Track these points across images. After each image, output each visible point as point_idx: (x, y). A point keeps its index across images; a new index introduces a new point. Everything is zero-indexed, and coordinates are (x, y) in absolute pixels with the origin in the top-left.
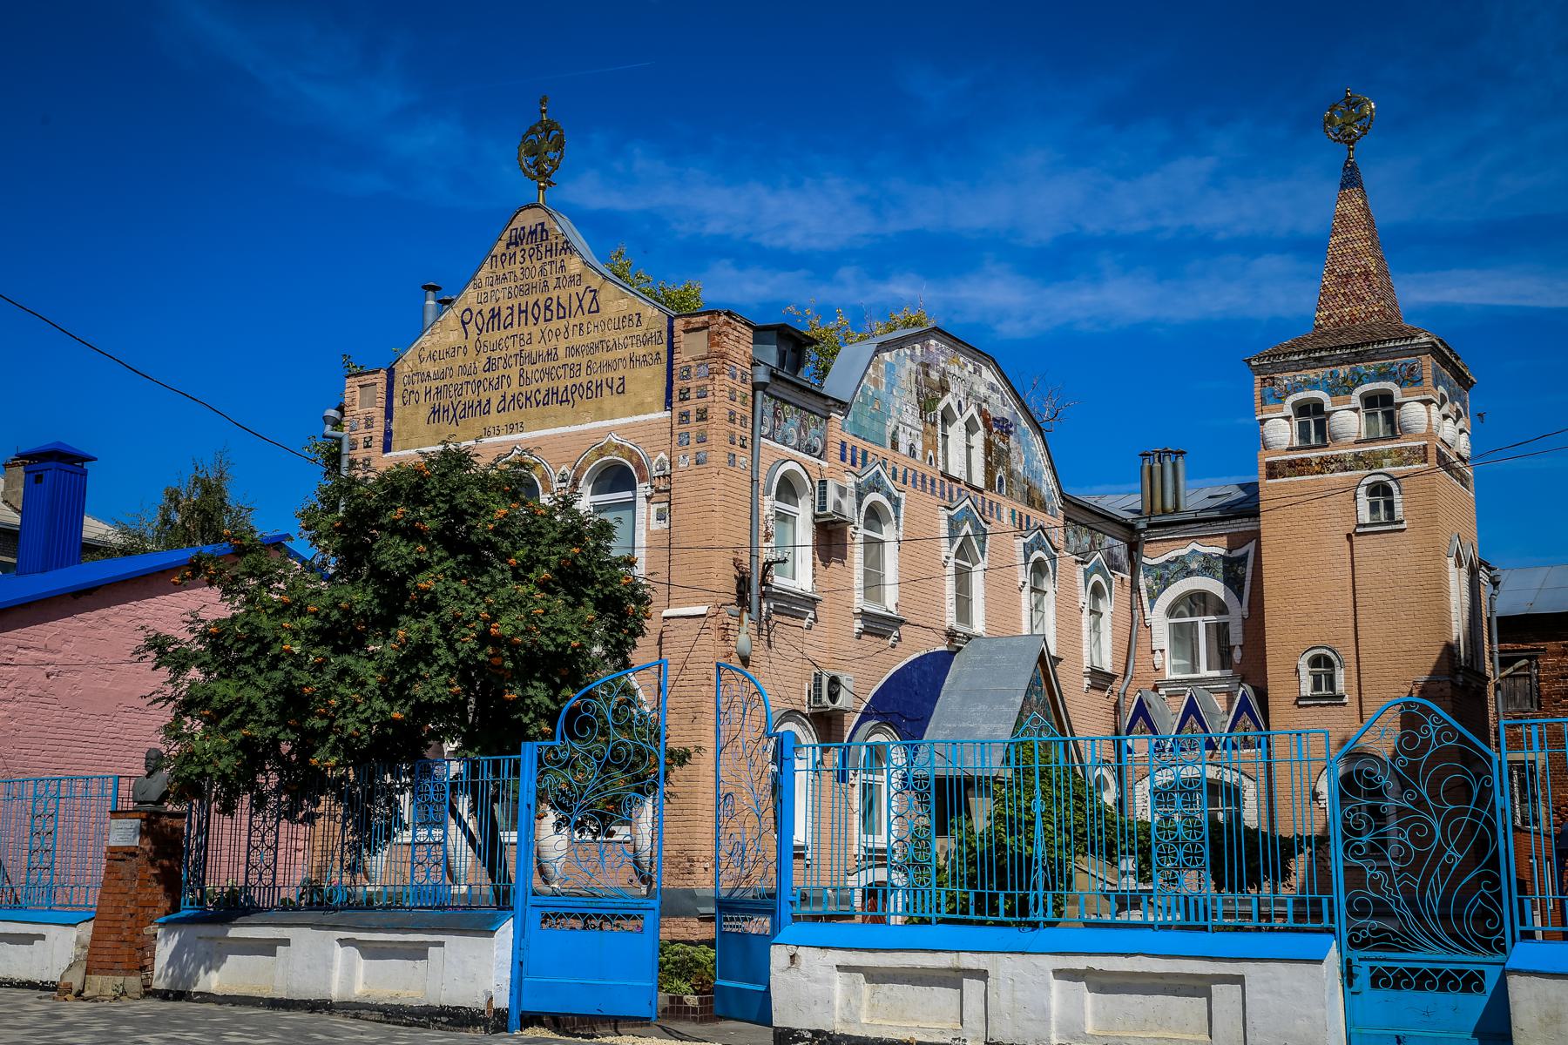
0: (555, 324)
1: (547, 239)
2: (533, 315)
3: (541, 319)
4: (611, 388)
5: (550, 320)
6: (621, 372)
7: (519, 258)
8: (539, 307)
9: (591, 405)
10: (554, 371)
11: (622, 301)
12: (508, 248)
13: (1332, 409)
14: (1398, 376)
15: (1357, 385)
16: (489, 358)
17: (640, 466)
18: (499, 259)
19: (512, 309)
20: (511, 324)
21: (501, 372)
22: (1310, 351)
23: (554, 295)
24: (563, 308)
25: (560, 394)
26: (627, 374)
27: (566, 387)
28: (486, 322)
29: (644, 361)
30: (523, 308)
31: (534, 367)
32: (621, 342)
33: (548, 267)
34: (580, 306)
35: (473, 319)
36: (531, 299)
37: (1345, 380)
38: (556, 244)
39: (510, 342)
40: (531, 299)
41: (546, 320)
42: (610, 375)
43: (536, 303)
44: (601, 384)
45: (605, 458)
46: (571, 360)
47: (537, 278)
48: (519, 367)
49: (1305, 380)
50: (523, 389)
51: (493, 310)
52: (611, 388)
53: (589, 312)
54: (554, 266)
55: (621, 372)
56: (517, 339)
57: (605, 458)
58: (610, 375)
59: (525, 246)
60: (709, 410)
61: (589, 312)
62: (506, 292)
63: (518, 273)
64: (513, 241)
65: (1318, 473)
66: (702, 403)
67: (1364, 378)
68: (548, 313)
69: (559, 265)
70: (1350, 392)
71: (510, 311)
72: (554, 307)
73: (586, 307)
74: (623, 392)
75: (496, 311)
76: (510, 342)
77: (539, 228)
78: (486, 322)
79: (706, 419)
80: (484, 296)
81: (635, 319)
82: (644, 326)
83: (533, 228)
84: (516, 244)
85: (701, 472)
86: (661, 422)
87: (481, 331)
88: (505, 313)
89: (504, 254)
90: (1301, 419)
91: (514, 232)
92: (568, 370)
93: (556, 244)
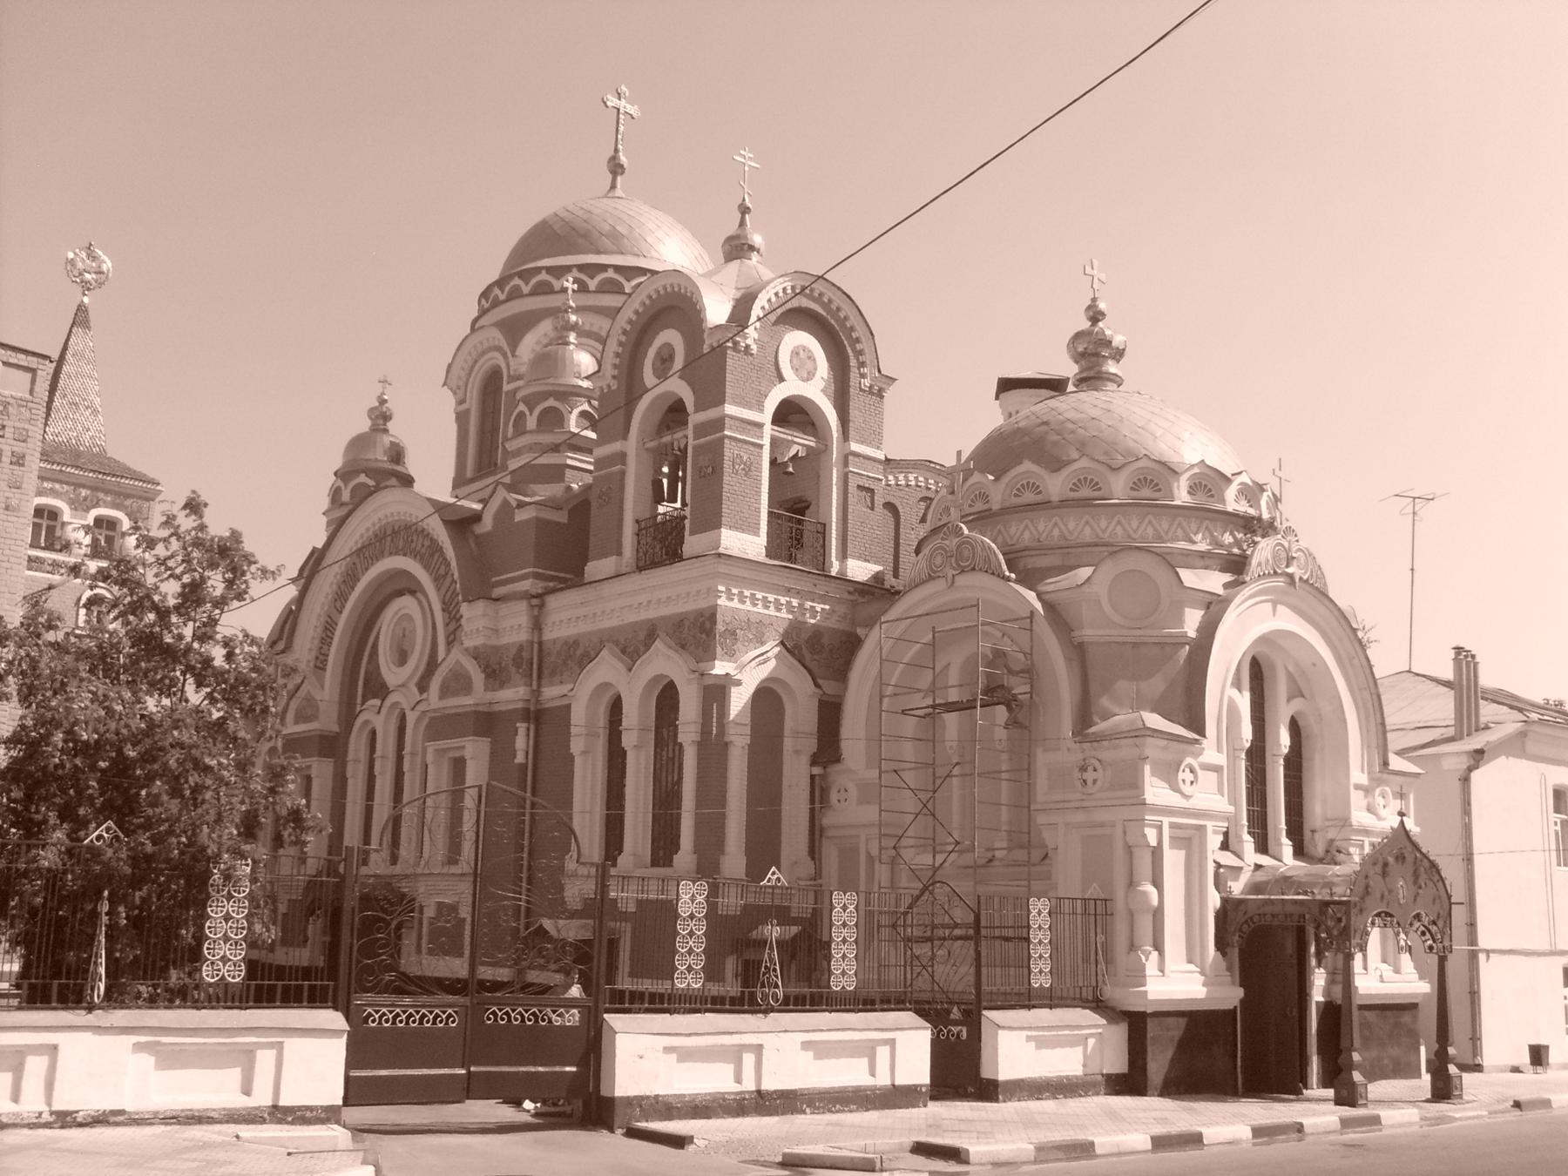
13: (70, 520)
14: (129, 510)
15: (94, 507)
22: (64, 465)
37: (85, 499)
49: (51, 489)
65: (48, 572)
66: (19, 448)
67: (101, 503)
70: (88, 510)
79: (23, 465)
85: (10, 518)
90: (36, 520)
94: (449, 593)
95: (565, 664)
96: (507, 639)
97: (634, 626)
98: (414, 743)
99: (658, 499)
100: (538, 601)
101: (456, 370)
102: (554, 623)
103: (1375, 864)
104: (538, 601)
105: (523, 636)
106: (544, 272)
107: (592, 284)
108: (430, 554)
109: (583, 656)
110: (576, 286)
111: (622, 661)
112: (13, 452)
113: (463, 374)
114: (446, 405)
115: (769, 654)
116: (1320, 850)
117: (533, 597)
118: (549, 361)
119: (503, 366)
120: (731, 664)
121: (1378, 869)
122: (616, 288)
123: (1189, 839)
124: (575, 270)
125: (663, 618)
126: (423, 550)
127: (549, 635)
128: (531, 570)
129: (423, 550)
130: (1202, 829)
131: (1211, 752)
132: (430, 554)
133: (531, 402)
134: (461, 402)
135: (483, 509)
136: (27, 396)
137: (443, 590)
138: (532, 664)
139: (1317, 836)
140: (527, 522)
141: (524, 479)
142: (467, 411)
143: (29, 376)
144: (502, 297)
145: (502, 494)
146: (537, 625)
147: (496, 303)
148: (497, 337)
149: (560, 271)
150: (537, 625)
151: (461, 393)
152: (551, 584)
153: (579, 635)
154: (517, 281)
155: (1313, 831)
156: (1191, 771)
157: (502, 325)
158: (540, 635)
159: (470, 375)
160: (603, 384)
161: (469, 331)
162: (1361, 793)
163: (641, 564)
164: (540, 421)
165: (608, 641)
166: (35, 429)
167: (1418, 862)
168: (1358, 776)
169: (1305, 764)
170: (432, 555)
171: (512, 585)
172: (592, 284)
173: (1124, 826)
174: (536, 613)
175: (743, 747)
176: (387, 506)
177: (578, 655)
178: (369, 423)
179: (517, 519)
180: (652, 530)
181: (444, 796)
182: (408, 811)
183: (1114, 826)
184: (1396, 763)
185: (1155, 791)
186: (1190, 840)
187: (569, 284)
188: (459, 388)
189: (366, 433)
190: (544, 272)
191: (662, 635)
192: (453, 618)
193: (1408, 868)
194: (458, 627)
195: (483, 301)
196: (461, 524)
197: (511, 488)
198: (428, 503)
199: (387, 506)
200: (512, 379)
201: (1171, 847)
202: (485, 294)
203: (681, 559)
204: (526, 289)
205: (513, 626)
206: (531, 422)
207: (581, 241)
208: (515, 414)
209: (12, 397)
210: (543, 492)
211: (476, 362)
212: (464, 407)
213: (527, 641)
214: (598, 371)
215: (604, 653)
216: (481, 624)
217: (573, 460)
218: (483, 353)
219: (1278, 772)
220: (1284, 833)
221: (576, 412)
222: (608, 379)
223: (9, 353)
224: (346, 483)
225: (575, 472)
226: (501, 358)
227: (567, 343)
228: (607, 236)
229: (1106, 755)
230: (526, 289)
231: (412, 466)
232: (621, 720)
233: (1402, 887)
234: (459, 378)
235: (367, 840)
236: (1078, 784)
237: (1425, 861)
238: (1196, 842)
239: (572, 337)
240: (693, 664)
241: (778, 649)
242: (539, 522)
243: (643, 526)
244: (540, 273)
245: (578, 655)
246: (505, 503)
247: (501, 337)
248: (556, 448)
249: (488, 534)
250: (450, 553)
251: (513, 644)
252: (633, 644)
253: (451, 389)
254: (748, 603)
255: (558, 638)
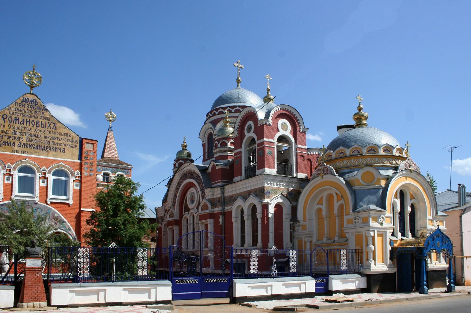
0: (40, 128)
1: (37, 105)
2: (34, 123)
3: (35, 126)
4: (61, 150)
5: (39, 127)
6: (64, 147)
7: (26, 106)
8: (34, 122)
9: (53, 153)
10: (40, 141)
11: (64, 129)
12: (22, 102)
16: (14, 131)
17: (72, 173)
18: (18, 104)
19: (24, 119)
20: (23, 124)
21: (19, 136)
23: (41, 120)
24: (43, 125)
25: (42, 147)
26: (66, 148)
27: (44, 147)
28: (13, 120)
29: (72, 146)
30: (28, 120)
31: (32, 138)
32: (64, 140)
33: (38, 113)
34: (50, 126)
35: (8, 118)
36: (32, 119)
38: (41, 107)
39: (22, 128)
40: (32, 119)
41: (37, 126)
42: (60, 147)
43: (33, 121)
44: (57, 148)
45: (60, 168)
46: (46, 140)
47: (33, 114)
48: (26, 137)
50: (28, 143)
51: (16, 118)
52: (61, 150)
53: (53, 129)
54: (40, 113)
55: (64, 147)
56: (26, 129)
57: (60, 168)
58: (60, 147)
59: (30, 105)
60: (94, 163)
61: (53, 129)
62: (21, 115)
63: (26, 111)
64: (24, 100)
68: (38, 125)
69: (42, 113)
71: (23, 120)
72: (40, 123)
73: (52, 127)
74: (65, 152)
75: (17, 118)
76: (23, 129)
77: (34, 101)
78: (13, 120)
79: (93, 165)
80: (12, 113)
81: (69, 135)
82: (72, 138)
83: (32, 100)
84: (26, 102)
86: (76, 162)
87: (11, 122)
88: (20, 120)
89: (20, 103)
91: (24, 99)
92: (45, 142)
93: (41, 107)
94: (202, 187)
95: (230, 201)
96: (216, 197)
97: (246, 192)
98: (190, 222)
99: (250, 161)
100: (223, 188)
101: (201, 133)
102: (227, 192)
103: (430, 238)
104: (223, 188)
105: (220, 196)
106: (221, 109)
107: (233, 111)
108: (197, 178)
109: (234, 199)
110: (228, 112)
111: (243, 200)
112: (90, 163)
113: (203, 135)
114: (200, 142)
115: (278, 197)
116: (419, 235)
117: (221, 186)
118: (222, 130)
119: (212, 131)
120: (269, 199)
121: (432, 239)
122: (238, 111)
123: (383, 234)
124: (228, 108)
125: (251, 190)
126: (195, 177)
127: (226, 195)
128: (220, 180)
129: (195, 177)
130: (386, 232)
131: (388, 213)
132: (197, 178)
133: (218, 140)
134: (203, 141)
135: (209, 166)
136: (92, 150)
137: (200, 186)
138: (222, 202)
139: (418, 232)
140: (219, 169)
141: (218, 159)
142: (205, 143)
143: (92, 145)
144: (211, 116)
145: (213, 163)
146: (223, 193)
147: (210, 117)
148: (210, 125)
149: (224, 108)
150: (223, 193)
151: (203, 139)
152: (226, 183)
153: (233, 195)
154: (214, 111)
155: (417, 231)
156: (383, 218)
157: (211, 122)
158: (224, 195)
159: (205, 135)
160: (235, 135)
161: (204, 124)
162: (430, 221)
163: (246, 177)
164: (221, 145)
165: (240, 196)
166: (94, 157)
167: (443, 237)
168: (429, 217)
169: (415, 214)
170: (198, 178)
171: (217, 184)
172: (233, 111)
173: (365, 232)
174: (222, 190)
175: (273, 219)
176: (187, 167)
177: (232, 199)
178: (182, 148)
179: (217, 169)
180: (248, 169)
181: (191, 234)
182: (184, 238)
183: (363, 232)
184: (440, 213)
185: (373, 224)
186: (382, 235)
187: (226, 111)
188: (202, 138)
189: (181, 151)
190: (221, 109)
191: (252, 194)
192: (203, 193)
193: (440, 239)
194: (204, 195)
195: (207, 117)
196: (203, 170)
197: (215, 161)
198: (196, 167)
199: (187, 167)
200: (215, 135)
201: (377, 236)
202: (207, 115)
203: (256, 176)
204: (217, 113)
205: (217, 193)
206: (219, 145)
207: (230, 100)
208: (215, 143)
209: (89, 150)
210: (223, 162)
211: (206, 132)
212: (204, 142)
213: (221, 197)
214: (233, 132)
215: (239, 198)
216: (209, 193)
217: (230, 154)
218: (207, 130)
219: (408, 217)
220: (409, 231)
221: (230, 142)
222: (236, 134)
223: (87, 140)
224: (177, 162)
225: (230, 157)
226: (212, 130)
227: (227, 126)
228: (230, 99)
229: (361, 216)
230: (217, 113)
231: (193, 157)
232: (243, 214)
233: (438, 243)
234: (202, 136)
235: (173, 244)
236: (354, 223)
237: (445, 236)
238: (384, 235)
239: (228, 124)
240: (259, 200)
241: (280, 195)
242: (221, 168)
243: (247, 168)
244: (220, 109)
245: (232, 199)
246: (214, 165)
247: (212, 126)
248: (225, 151)
249: (210, 172)
250: (201, 178)
251: (218, 198)
252: (245, 196)
253: (200, 139)
254: (272, 185)
255: (228, 196)
